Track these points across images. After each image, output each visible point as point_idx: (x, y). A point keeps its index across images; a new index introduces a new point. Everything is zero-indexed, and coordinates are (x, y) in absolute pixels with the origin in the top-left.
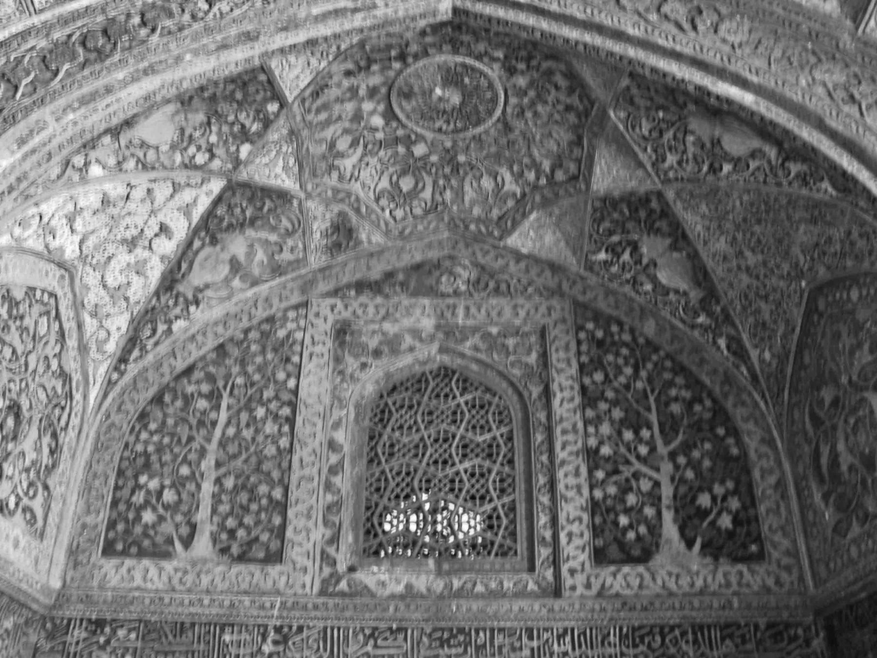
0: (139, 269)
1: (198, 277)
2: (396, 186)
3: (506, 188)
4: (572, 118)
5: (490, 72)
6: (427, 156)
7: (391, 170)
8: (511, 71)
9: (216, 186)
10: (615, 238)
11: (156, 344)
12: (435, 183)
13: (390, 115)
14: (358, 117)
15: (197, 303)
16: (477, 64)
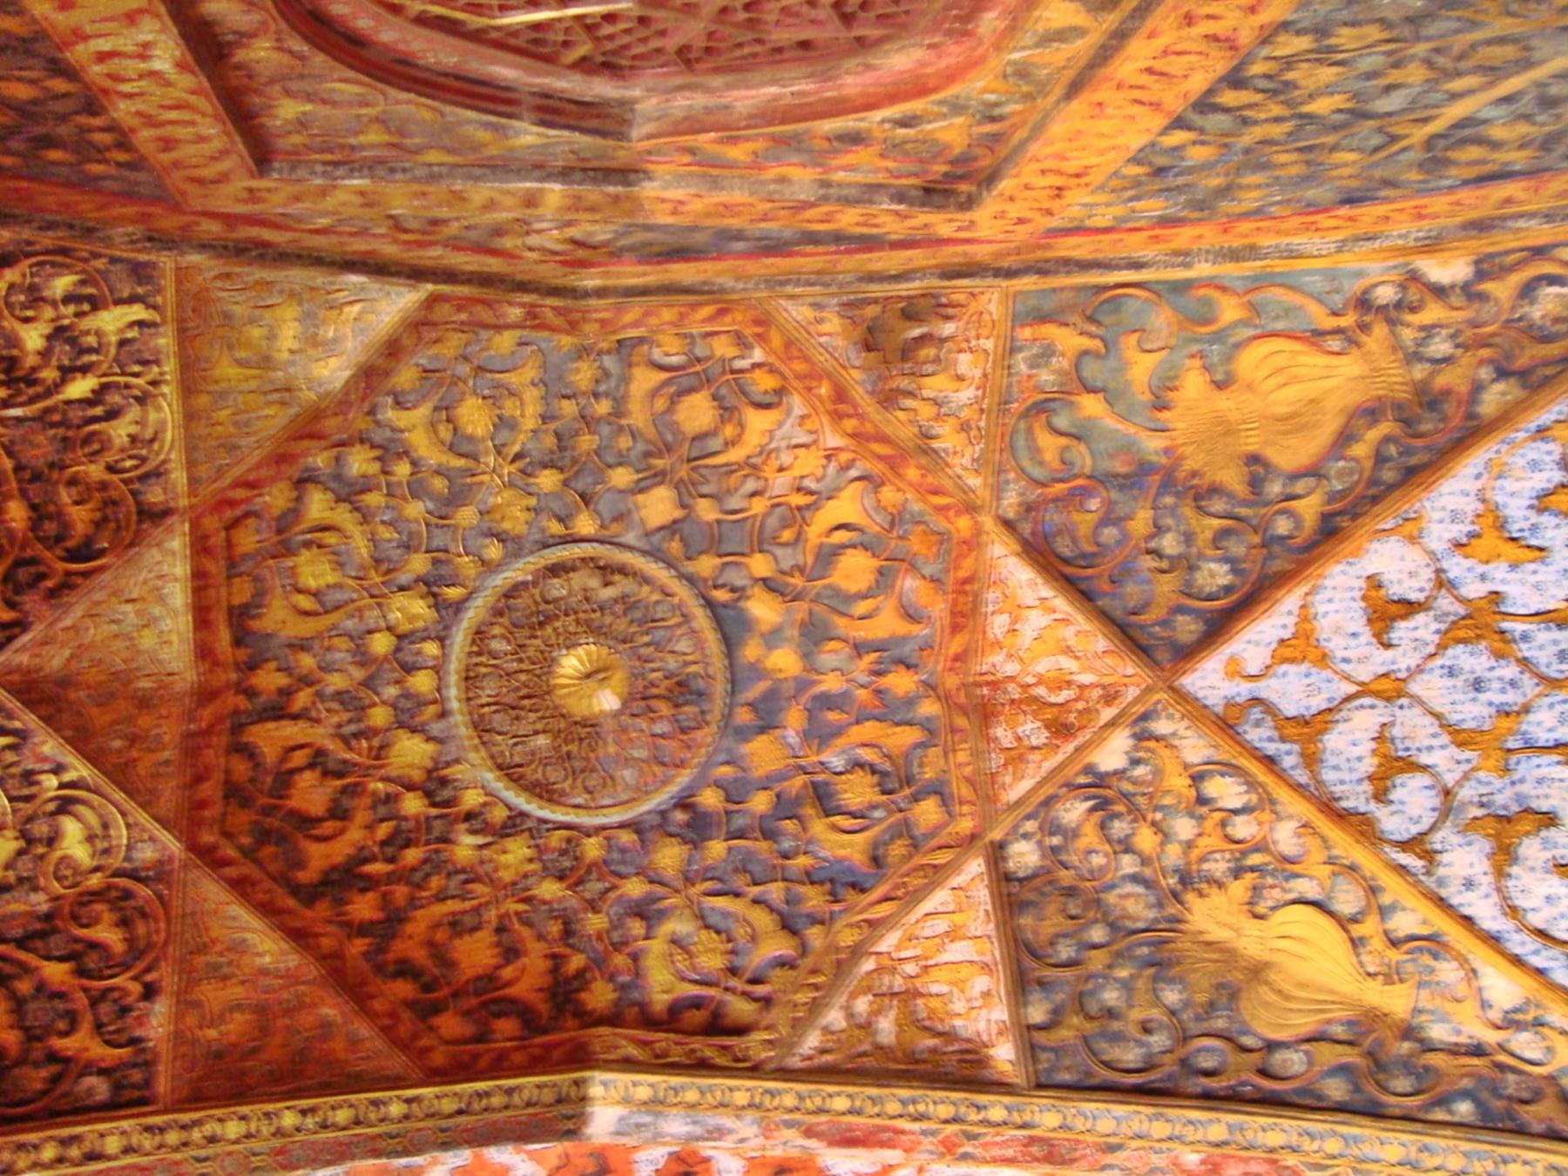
0: (1491, 531)
1: (1337, 379)
2: (727, 412)
3: (423, 412)
4: (269, 680)
5: (491, 778)
6: (639, 489)
7: (735, 455)
8: (435, 784)
9: (1208, 679)
10: (80, 388)
11: (1539, 252)
12: (618, 412)
13: (730, 626)
14: (813, 635)
15: (1363, 303)
16: (521, 802)
